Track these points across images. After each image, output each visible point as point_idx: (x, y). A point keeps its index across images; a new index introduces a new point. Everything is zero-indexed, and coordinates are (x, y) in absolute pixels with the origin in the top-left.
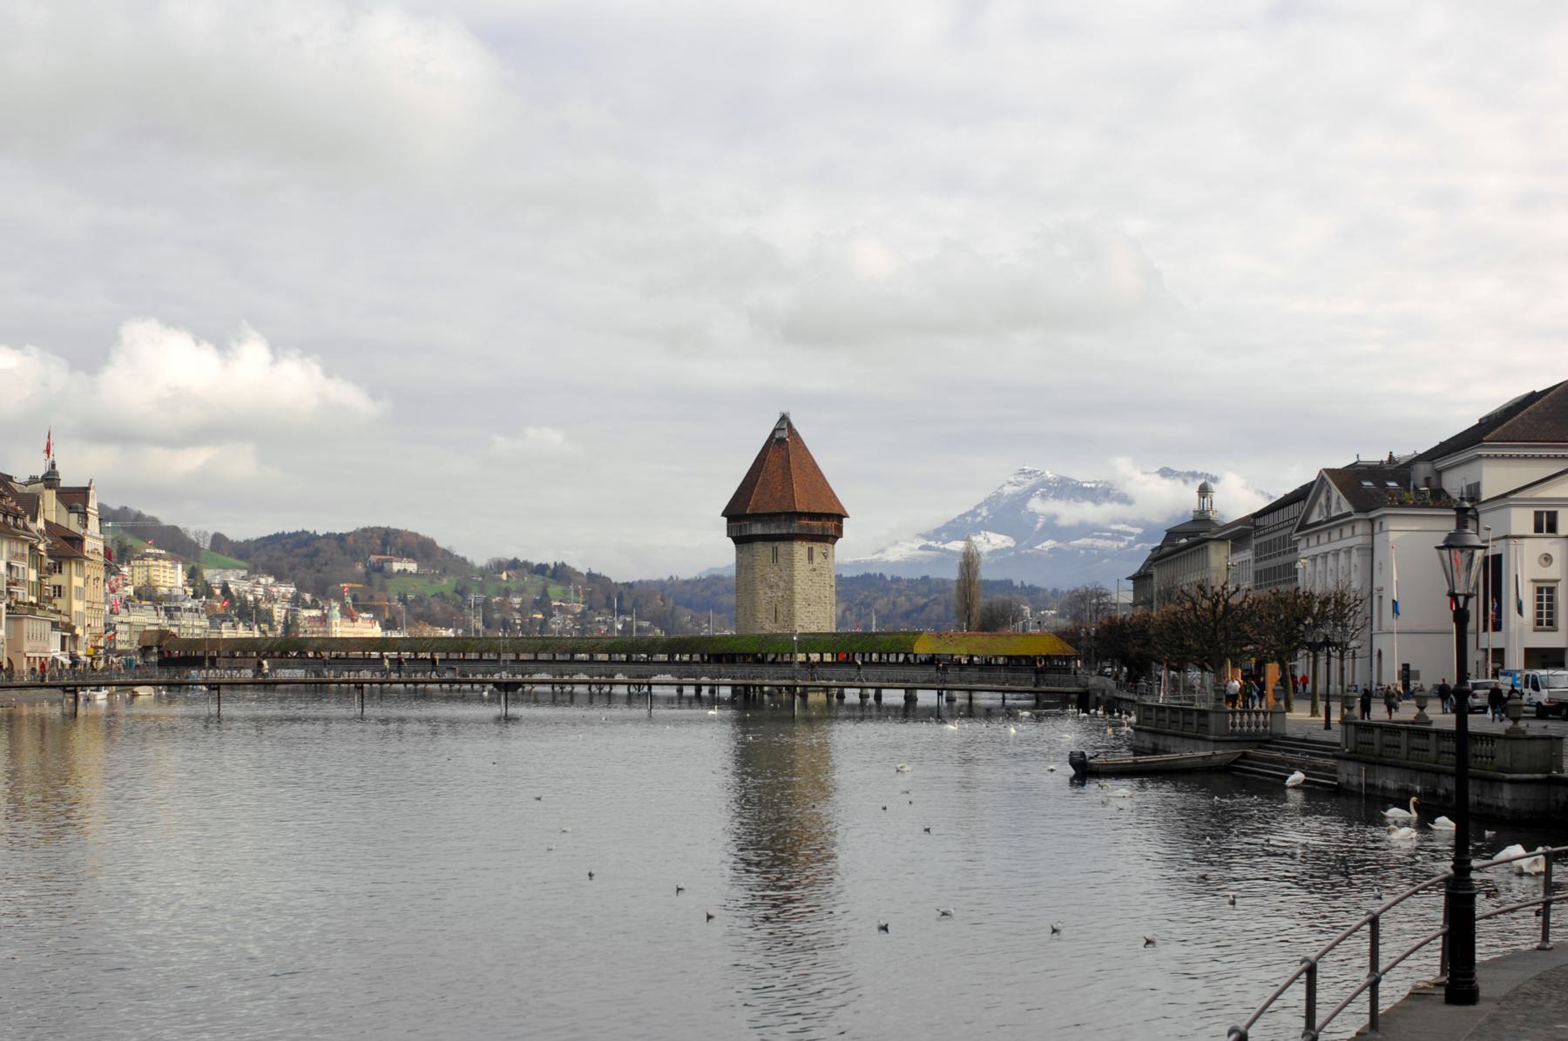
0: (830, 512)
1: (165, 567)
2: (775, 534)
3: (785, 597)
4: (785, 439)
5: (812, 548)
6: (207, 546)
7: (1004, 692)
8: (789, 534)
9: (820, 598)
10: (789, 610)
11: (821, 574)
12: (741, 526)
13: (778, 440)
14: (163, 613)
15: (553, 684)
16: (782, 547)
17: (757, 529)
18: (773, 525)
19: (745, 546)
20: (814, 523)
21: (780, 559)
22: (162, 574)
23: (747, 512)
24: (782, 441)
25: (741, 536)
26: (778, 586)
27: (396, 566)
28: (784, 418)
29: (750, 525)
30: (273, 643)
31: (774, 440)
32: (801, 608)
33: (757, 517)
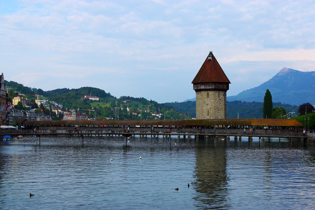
4: (211, 59)
7: (280, 137)
10: (213, 112)
12: (198, 86)
13: (209, 60)
15: (140, 134)
16: (211, 93)
17: (203, 87)
18: (207, 86)
19: (199, 93)
20: (220, 85)
22: (23, 101)
24: (210, 60)
25: (197, 89)
31: (208, 60)
33: (202, 83)
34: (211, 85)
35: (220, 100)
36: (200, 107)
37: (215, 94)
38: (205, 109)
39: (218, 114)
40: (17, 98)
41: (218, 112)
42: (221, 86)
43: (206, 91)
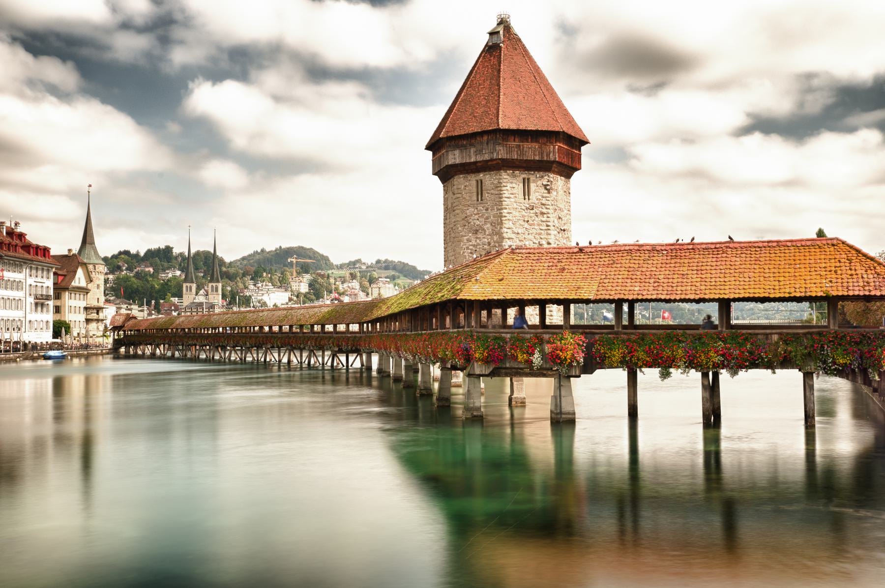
0: (550, 129)
3: (492, 244)
5: (528, 179)
8: (492, 160)
11: (542, 214)
16: (488, 179)
17: (454, 157)
18: (472, 150)
19: (449, 184)
20: (527, 145)
21: (486, 195)
23: (441, 136)
26: (484, 229)
28: (503, 23)
29: (447, 152)
31: (487, 48)
34: (487, 144)
37: (506, 186)
38: (468, 248)
42: (531, 151)
43: (473, 175)
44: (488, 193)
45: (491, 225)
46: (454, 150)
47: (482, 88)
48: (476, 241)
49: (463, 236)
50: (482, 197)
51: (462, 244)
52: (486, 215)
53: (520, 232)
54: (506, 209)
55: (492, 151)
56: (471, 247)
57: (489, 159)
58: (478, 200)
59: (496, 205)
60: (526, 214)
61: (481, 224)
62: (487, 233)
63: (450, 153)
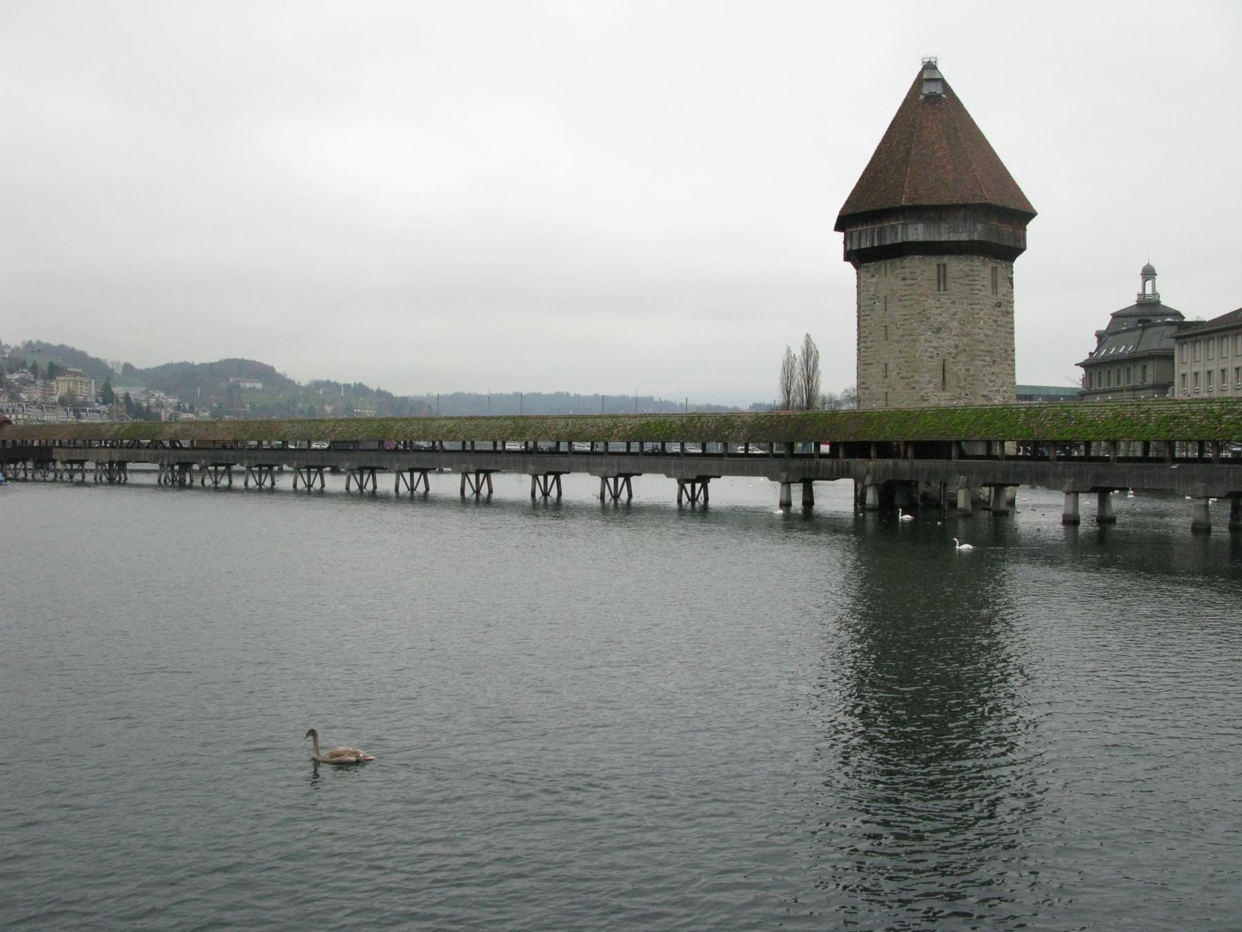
1: (81, 382)
2: (949, 242)
3: (961, 347)
4: (939, 96)
6: (120, 371)
8: (971, 242)
9: (1006, 351)
10: (967, 370)
13: (928, 97)
14: (72, 413)
16: (956, 266)
17: (917, 232)
18: (944, 226)
21: (950, 284)
22: (79, 387)
23: (903, 203)
24: (933, 99)
25: (881, 247)
27: (248, 385)
29: (905, 226)
30: (120, 429)
31: (922, 97)
32: (984, 366)
34: (965, 220)
35: (999, 305)
36: (898, 342)
38: (926, 351)
39: (991, 381)
40: (64, 378)
41: (993, 373)
44: (956, 283)
45: (960, 323)
46: (917, 223)
47: (938, 148)
48: (937, 342)
49: (919, 334)
50: (945, 286)
51: (918, 344)
52: (953, 310)
53: (990, 333)
54: (978, 304)
55: (972, 230)
56: (930, 350)
57: (968, 239)
58: (939, 290)
59: (966, 298)
60: (994, 313)
61: (944, 321)
62: (953, 333)
63: (910, 226)
